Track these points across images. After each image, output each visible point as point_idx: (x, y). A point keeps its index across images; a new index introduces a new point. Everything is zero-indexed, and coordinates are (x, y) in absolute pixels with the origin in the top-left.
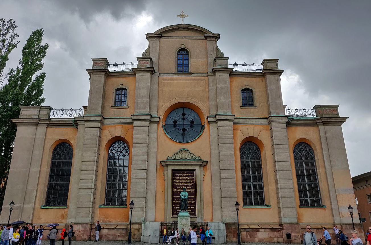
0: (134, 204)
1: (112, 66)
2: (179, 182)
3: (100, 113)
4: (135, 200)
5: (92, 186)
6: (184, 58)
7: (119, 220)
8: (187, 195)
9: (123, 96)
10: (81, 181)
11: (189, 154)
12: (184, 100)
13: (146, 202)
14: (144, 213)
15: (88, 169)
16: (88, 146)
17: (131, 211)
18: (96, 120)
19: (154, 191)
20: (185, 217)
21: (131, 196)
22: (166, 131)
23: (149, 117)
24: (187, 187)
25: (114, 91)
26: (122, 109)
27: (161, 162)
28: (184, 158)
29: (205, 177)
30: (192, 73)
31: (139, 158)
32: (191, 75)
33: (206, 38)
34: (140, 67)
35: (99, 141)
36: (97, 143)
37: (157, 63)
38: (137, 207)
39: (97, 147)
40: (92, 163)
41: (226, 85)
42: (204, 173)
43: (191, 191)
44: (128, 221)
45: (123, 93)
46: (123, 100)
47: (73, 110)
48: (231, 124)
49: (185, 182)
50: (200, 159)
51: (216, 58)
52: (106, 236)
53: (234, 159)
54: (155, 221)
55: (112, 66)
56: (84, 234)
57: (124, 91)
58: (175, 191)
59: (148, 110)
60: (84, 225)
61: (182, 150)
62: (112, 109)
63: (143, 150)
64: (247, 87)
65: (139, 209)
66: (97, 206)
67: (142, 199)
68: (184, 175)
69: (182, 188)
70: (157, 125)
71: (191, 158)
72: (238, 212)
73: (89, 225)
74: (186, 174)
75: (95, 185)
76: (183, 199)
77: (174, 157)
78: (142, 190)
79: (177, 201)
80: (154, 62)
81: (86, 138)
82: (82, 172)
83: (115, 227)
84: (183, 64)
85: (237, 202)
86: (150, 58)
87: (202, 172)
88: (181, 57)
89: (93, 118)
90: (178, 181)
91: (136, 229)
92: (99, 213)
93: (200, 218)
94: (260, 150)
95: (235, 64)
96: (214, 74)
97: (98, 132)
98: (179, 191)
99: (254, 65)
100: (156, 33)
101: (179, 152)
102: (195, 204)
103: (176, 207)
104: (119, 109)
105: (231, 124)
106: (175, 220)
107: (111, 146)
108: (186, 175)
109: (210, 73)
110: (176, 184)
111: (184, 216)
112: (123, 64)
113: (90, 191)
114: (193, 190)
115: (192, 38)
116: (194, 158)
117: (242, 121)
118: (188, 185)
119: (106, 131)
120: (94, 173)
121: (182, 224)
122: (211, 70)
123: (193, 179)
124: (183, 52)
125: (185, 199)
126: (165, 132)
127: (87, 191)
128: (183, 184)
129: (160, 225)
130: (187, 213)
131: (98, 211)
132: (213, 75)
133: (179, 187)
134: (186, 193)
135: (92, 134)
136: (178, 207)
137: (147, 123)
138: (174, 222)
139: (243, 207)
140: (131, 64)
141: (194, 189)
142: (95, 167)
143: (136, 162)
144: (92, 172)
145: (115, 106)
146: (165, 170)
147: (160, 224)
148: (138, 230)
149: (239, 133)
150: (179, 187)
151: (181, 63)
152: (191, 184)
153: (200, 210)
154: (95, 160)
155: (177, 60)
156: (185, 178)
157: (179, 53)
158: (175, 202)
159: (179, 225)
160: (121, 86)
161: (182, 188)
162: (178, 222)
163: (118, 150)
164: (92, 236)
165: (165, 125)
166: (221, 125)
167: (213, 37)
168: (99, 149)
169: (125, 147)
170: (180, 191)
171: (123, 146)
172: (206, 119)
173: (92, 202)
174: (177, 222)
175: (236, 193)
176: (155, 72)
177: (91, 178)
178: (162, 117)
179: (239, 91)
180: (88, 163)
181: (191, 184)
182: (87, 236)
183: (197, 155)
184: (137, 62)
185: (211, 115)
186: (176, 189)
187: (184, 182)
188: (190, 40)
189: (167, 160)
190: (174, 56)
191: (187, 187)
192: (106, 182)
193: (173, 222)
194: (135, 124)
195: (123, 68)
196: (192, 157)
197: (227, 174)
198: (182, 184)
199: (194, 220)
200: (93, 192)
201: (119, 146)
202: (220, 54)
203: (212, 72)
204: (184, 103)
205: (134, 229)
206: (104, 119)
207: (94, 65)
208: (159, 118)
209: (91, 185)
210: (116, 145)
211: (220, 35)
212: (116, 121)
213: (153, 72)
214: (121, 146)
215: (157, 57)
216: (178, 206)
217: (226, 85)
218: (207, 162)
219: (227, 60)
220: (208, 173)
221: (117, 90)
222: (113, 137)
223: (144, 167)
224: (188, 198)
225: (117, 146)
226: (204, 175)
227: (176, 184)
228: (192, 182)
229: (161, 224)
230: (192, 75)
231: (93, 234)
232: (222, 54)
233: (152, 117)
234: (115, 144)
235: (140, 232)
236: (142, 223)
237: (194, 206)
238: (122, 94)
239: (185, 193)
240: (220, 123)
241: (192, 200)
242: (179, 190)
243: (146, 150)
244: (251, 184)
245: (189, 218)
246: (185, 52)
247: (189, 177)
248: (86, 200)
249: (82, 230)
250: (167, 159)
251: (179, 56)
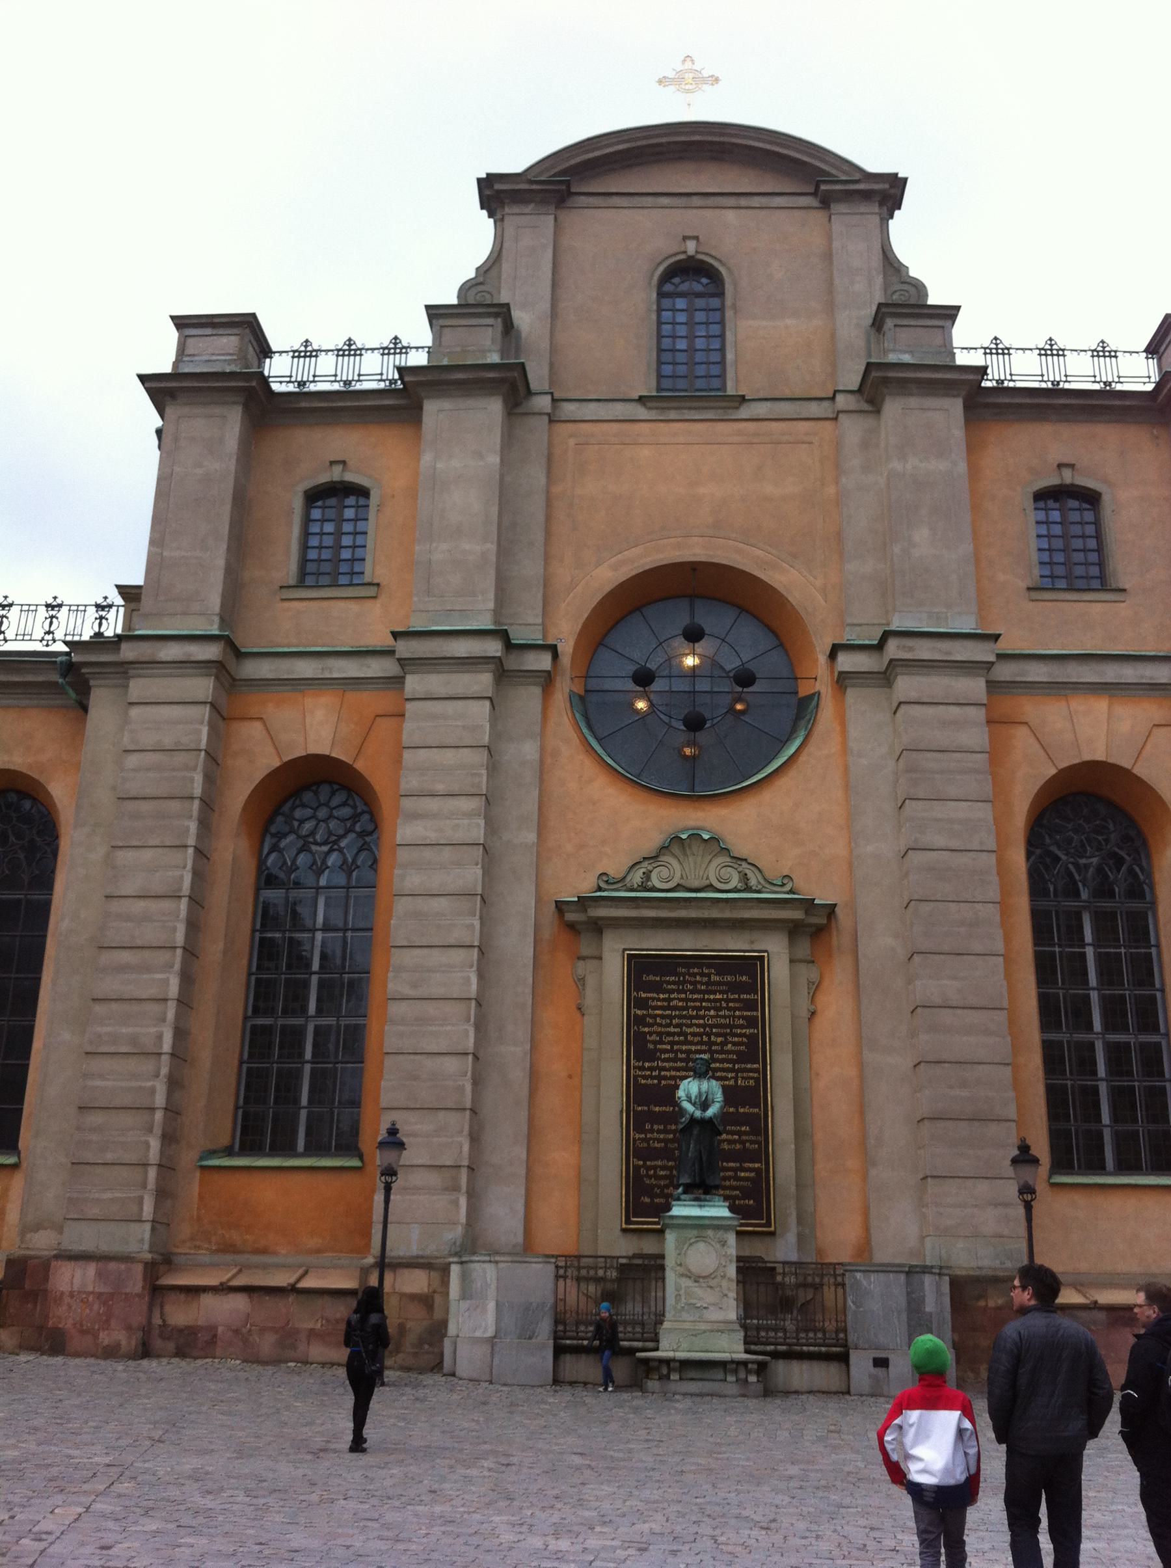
0: (401, 1145)
1: (287, 358)
2: (668, 1025)
3: (217, 619)
4: (411, 1126)
5: (160, 1037)
6: (700, 316)
7: (314, 1242)
8: (719, 1096)
9: (347, 527)
10: (99, 1009)
11: (723, 859)
12: (696, 551)
13: (475, 1139)
14: (463, 1201)
15: (139, 943)
16: (145, 806)
17: (388, 1189)
18: (193, 659)
19: (518, 1075)
20: (710, 1233)
21: (384, 1101)
22: (590, 727)
23: (494, 648)
24: (712, 1052)
25: (298, 503)
26: (342, 604)
27: (560, 906)
28: (696, 884)
29: (822, 999)
30: (743, 399)
31: (437, 880)
32: (737, 408)
33: (826, 202)
34: (445, 362)
35: (209, 779)
36: (198, 791)
37: (545, 345)
38: (420, 1162)
39: (195, 813)
40: (166, 905)
41: (942, 466)
42: (814, 976)
43: (736, 1079)
44: (368, 1246)
45: (349, 513)
46: (346, 554)
47: (60, 606)
48: (975, 687)
49: (704, 1026)
51: (884, 310)
52: (237, 1332)
53: (994, 893)
54: (527, 1248)
55: (287, 358)
56: (108, 1321)
57: (351, 501)
58: (645, 1077)
59: (491, 605)
60: (112, 1266)
61: (684, 836)
62: (286, 604)
63: (459, 836)
64: (1068, 477)
65: (434, 1179)
66: (188, 1157)
67: (453, 1119)
68: (694, 983)
69: (682, 1060)
70: (537, 691)
71: (735, 882)
72: (1028, 1207)
73: (139, 1268)
74: (708, 975)
75: (180, 1034)
76: (693, 1120)
77: (637, 877)
78: (451, 1065)
79: (657, 1137)
80: (524, 335)
81: (133, 760)
82: (106, 958)
83: (292, 1280)
84: (691, 350)
85: (1024, 1148)
86: (503, 312)
87: (802, 969)
88: (678, 307)
89: (172, 652)
90: (662, 1017)
91: (413, 1297)
92: (201, 1197)
93: (791, 1237)
94: (1145, 843)
95: (998, 349)
96: (870, 401)
97: (200, 731)
98: (665, 1078)
99: (1103, 352)
100: (540, 174)
101: (664, 849)
102: (760, 1153)
103: (648, 1168)
104: (325, 604)
105: (975, 687)
106: (648, 1246)
107: (276, 812)
108: (708, 984)
109: (849, 396)
110: (651, 1034)
111: (699, 1226)
112: (350, 350)
113: (148, 1066)
114: (751, 1070)
115: (743, 202)
116: (753, 882)
117: (1037, 673)
118: (719, 1040)
119: (247, 724)
120: (177, 966)
121: (688, 1275)
122: (853, 381)
123: (750, 1005)
125: (707, 1125)
126: (585, 731)
127: (132, 1064)
128: (694, 1034)
129: (557, 1277)
130: (719, 1210)
131: (196, 1188)
132: (866, 407)
133: (666, 1051)
134: (714, 1088)
135: (168, 742)
136: (663, 1168)
137: (484, 681)
138: (639, 1261)
139: (1050, 1177)
140: (396, 347)
141: (755, 1066)
142: (181, 929)
143: (421, 904)
144: (163, 957)
145: (301, 583)
146: (585, 951)
147: (557, 1267)
148: (426, 1301)
149: (1021, 738)
150: (666, 1051)
151: (682, 344)
152: (740, 1035)
153: (793, 1188)
154: (180, 890)
155: (660, 323)
156: (703, 1000)
157: (668, 288)
158: (643, 1140)
159: (670, 1276)
160: (336, 474)
161: (682, 1060)
162: (662, 1257)
163: (313, 833)
164: (156, 1332)
165: (582, 693)
166: (913, 695)
167: (867, 195)
168: (205, 825)
169: (355, 817)
170: (673, 1073)
171: (346, 811)
172: (822, 659)
173: (158, 1130)
174: (659, 1262)
175: (1011, 1094)
176: (529, 393)
177: (152, 992)
178: (566, 648)
180: (142, 904)
181: (740, 1035)
182: (129, 1328)
183: (774, 866)
185: (851, 636)
186: (647, 1065)
187: (698, 1026)
188: (730, 215)
189: (599, 894)
190: (643, 298)
191: (717, 1052)
192: (246, 1018)
193: (635, 1256)
194: (414, 683)
195: (348, 368)
196: (745, 878)
197: (955, 978)
198: (685, 1034)
199: (756, 1249)
200: (164, 1071)
201: (322, 813)
202: (906, 287)
203: (860, 391)
204: (694, 568)
205: (403, 1295)
206: (239, 655)
207: (182, 351)
208: (553, 650)
209: (153, 1030)
210: (303, 806)
211: (905, 180)
212: (306, 669)
213: (522, 391)
214: (335, 813)
215: (545, 306)
216: (659, 1163)
217: (942, 466)
218: (831, 910)
219: (948, 323)
220: (838, 977)
221: (314, 496)
222: (286, 759)
223: (467, 928)
224: (723, 1116)
225: (308, 812)
226: (815, 988)
227: (651, 1034)
228: (741, 1022)
229: (561, 1272)
230: (745, 412)
231: (160, 1322)
232: (919, 288)
233: (509, 646)
234: (298, 802)
235: (438, 1315)
236: (450, 1263)
237: (757, 1165)
238: (340, 521)
239: (705, 1085)
240: (906, 685)
241: (745, 1133)
242: (668, 1070)
243: (476, 831)
244: (1092, 1046)
245: (731, 1238)
246: (704, 281)
247: (726, 992)
248: (128, 1119)
249: (101, 1294)
250: (600, 889)
251: (667, 303)
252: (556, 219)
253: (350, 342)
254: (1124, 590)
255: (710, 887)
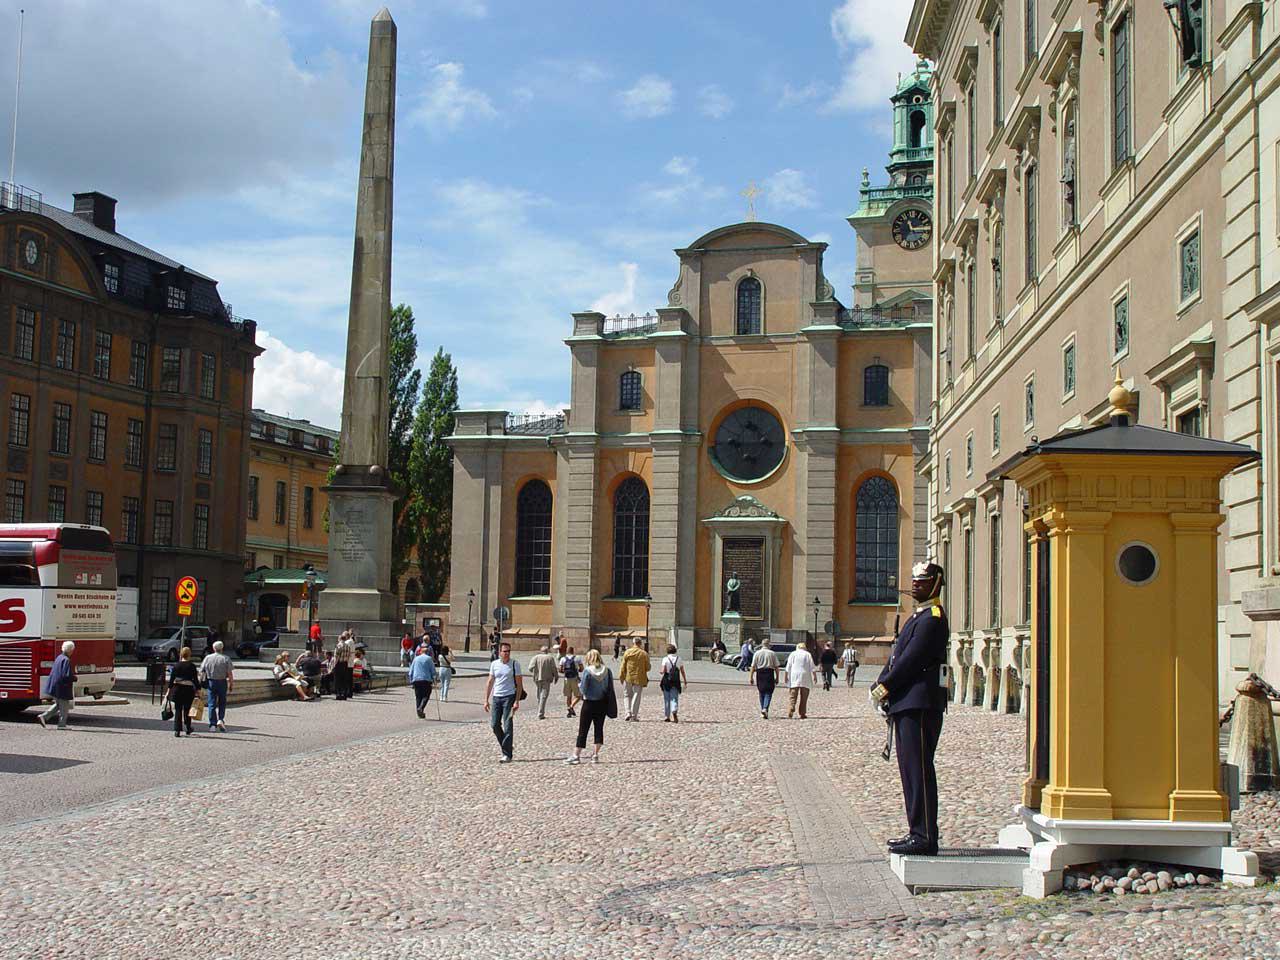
22: (716, 457)
25: (619, 379)
50: (776, 516)
57: (635, 375)
63: (671, 502)
77: (726, 513)
111: (730, 621)
112: (632, 318)
124: (749, 289)
130: (736, 615)
178: (706, 432)
179: (860, 371)
184: (657, 314)
252: (702, 263)
253: (632, 315)
254: (891, 406)
255: (748, 516)
